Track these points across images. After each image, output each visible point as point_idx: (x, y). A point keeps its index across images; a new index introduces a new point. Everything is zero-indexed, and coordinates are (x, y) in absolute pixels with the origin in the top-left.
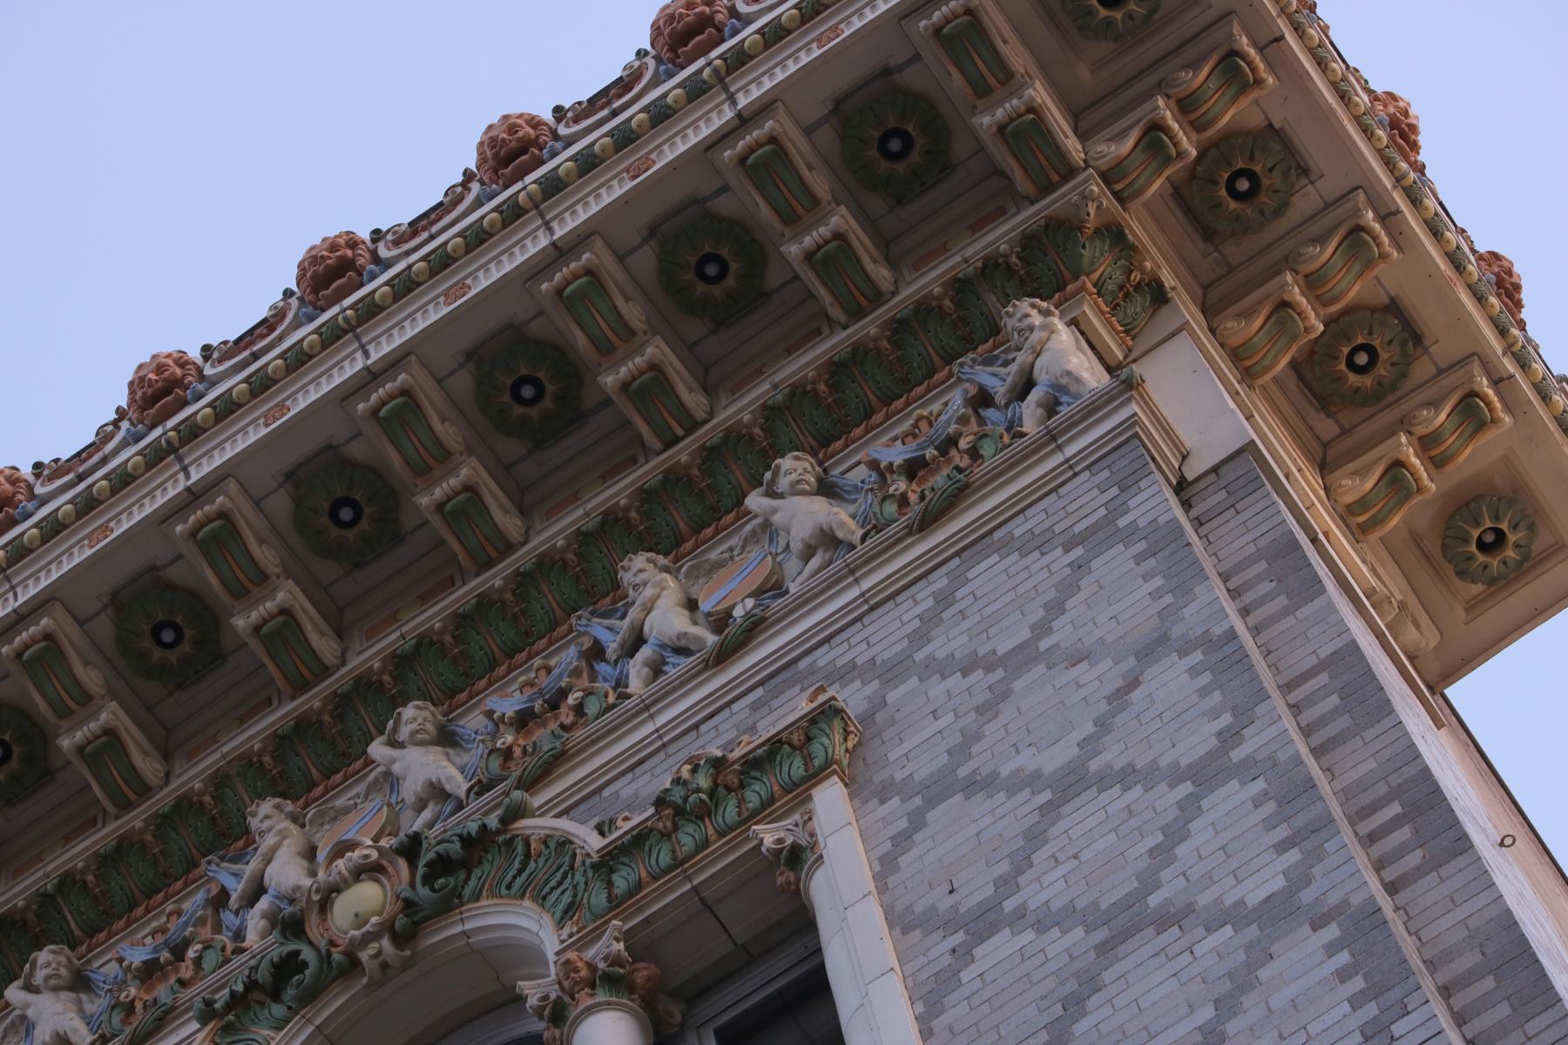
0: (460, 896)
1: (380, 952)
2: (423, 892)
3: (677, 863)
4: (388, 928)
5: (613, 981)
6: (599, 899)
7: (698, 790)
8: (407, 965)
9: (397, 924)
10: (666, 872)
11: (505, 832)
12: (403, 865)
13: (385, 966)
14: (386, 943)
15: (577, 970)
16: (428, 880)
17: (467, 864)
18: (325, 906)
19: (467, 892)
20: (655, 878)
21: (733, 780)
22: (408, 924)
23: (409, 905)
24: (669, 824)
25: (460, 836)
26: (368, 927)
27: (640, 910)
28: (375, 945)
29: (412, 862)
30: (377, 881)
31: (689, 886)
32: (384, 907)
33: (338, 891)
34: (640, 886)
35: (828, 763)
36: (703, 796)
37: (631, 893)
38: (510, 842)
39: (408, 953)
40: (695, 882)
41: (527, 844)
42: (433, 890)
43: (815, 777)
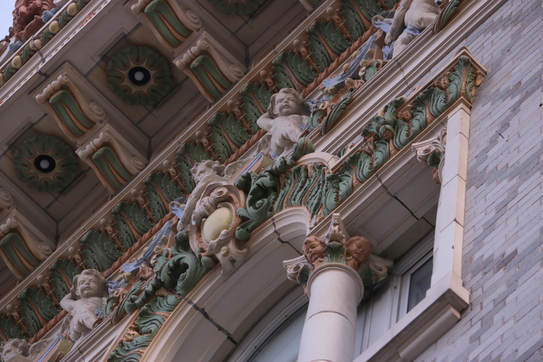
0: (271, 210)
1: (228, 252)
2: (251, 209)
3: (374, 170)
4: (231, 236)
5: (333, 250)
6: (330, 200)
7: (385, 123)
8: (246, 259)
9: (237, 232)
10: (367, 178)
11: (295, 165)
12: (241, 194)
13: (233, 261)
14: (231, 246)
15: (313, 247)
16: (252, 203)
17: (276, 189)
18: (199, 228)
19: (275, 206)
20: (362, 182)
21: (407, 114)
22: (244, 233)
23: (244, 220)
24: (371, 147)
25: (269, 172)
26: (220, 237)
27: (353, 204)
28: (224, 248)
29: (246, 193)
30: (228, 207)
31: (380, 185)
32: (230, 223)
33: (206, 217)
34: (353, 188)
35: (458, 96)
36: (388, 126)
37: (348, 193)
38: (298, 171)
39: (245, 250)
40: (383, 181)
41: (306, 170)
42: (256, 208)
43: (449, 106)
